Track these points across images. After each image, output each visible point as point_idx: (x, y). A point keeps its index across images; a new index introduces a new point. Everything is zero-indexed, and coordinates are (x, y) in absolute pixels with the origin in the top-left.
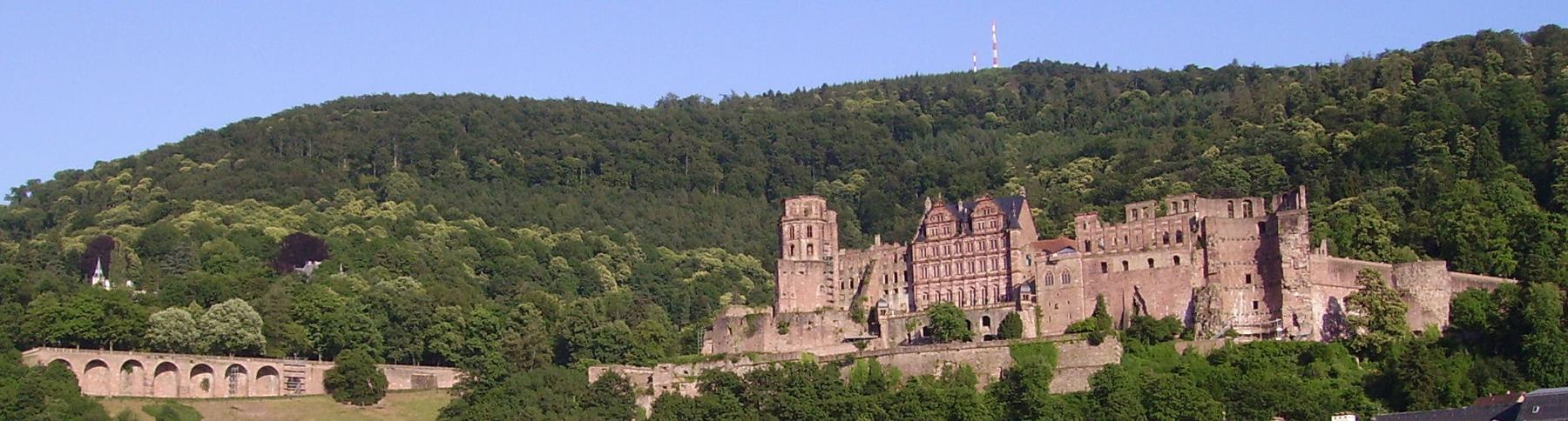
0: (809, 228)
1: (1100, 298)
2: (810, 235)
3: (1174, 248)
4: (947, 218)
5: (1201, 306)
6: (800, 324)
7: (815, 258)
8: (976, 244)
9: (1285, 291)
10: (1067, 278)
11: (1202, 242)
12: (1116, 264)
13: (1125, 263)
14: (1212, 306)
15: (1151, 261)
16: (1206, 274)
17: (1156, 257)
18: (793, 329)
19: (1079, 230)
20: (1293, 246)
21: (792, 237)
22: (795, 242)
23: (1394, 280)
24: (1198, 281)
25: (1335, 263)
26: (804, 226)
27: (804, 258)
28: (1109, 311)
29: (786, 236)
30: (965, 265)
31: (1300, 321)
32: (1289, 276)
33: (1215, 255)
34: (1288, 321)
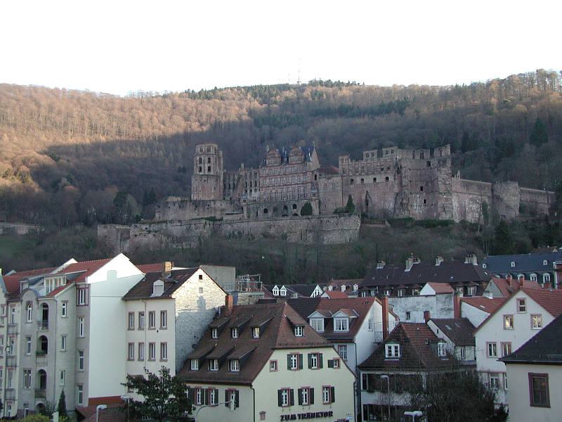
0: (209, 159)
1: (350, 197)
2: (209, 162)
6: (204, 206)
7: (212, 173)
12: (358, 180)
13: (363, 180)
14: (404, 201)
15: (375, 179)
19: (340, 163)
20: (443, 174)
21: (200, 162)
22: (202, 165)
23: (492, 190)
25: (463, 182)
27: (207, 173)
28: (354, 202)
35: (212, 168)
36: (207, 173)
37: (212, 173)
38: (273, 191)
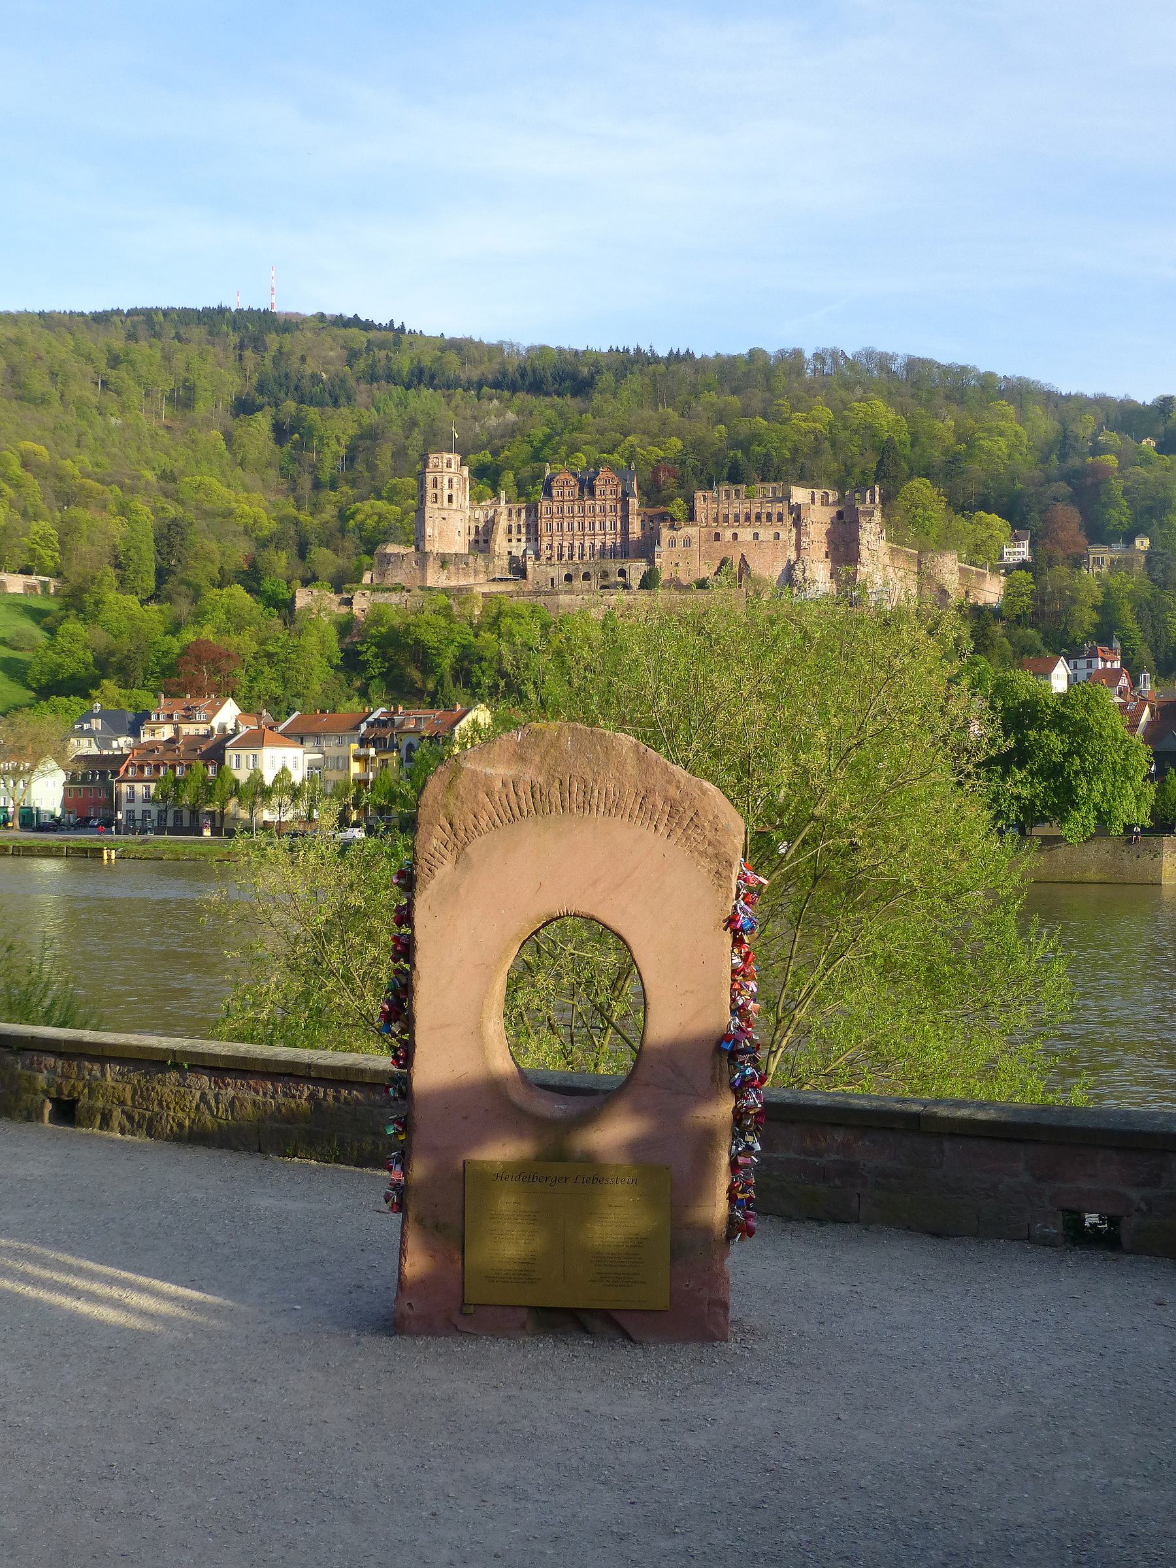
0: (450, 481)
2: (451, 486)
4: (572, 483)
5: (798, 574)
10: (687, 542)
11: (797, 522)
12: (728, 534)
13: (735, 536)
15: (756, 536)
16: (798, 548)
17: (761, 531)
21: (435, 485)
22: (438, 491)
24: (793, 557)
30: (587, 524)
32: (864, 554)
33: (808, 534)
35: (454, 498)
37: (454, 505)
38: (566, 544)
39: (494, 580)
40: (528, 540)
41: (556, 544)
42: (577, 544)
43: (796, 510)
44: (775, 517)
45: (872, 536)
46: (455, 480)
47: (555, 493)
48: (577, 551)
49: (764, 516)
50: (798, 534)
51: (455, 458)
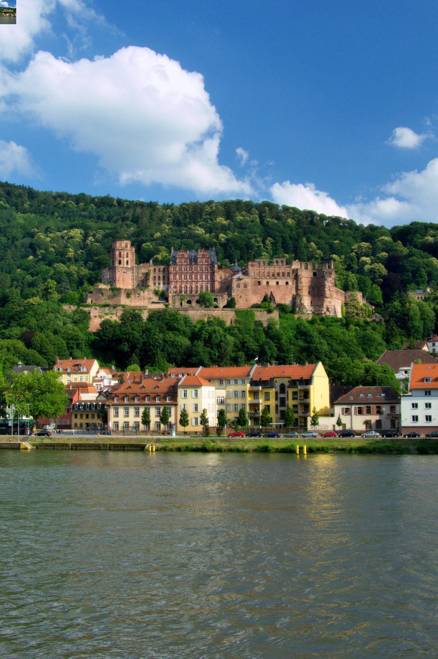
0: (127, 254)
2: (127, 257)
3: (287, 279)
4: (186, 256)
5: (298, 301)
8: (199, 268)
9: (325, 299)
10: (245, 286)
12: (264, 282)
13: (268, 283)
15: (277, 283)
18: (133, 296)
21: (120, 256)
22: (122, 259)
26: (125, 253)
27: (125, 266)
29: (117, 256)
31: (330, 310)
32: (328, 293)
33: (301, 283)
34: (325, 310)
36: (125, 266)
37: (129, 266)
38: (183, 286)
39: (153, 302)
40: (164, 284)
41: (178, 286)
42: (188, 286)
43: (295, 272)
44: (286, 274)
45: (330, 283)
46: (129, 254)
47: (178, 261)
48: (188, 289)
49: (286, 274)
50: (297, 283)
51: (129, 243)
